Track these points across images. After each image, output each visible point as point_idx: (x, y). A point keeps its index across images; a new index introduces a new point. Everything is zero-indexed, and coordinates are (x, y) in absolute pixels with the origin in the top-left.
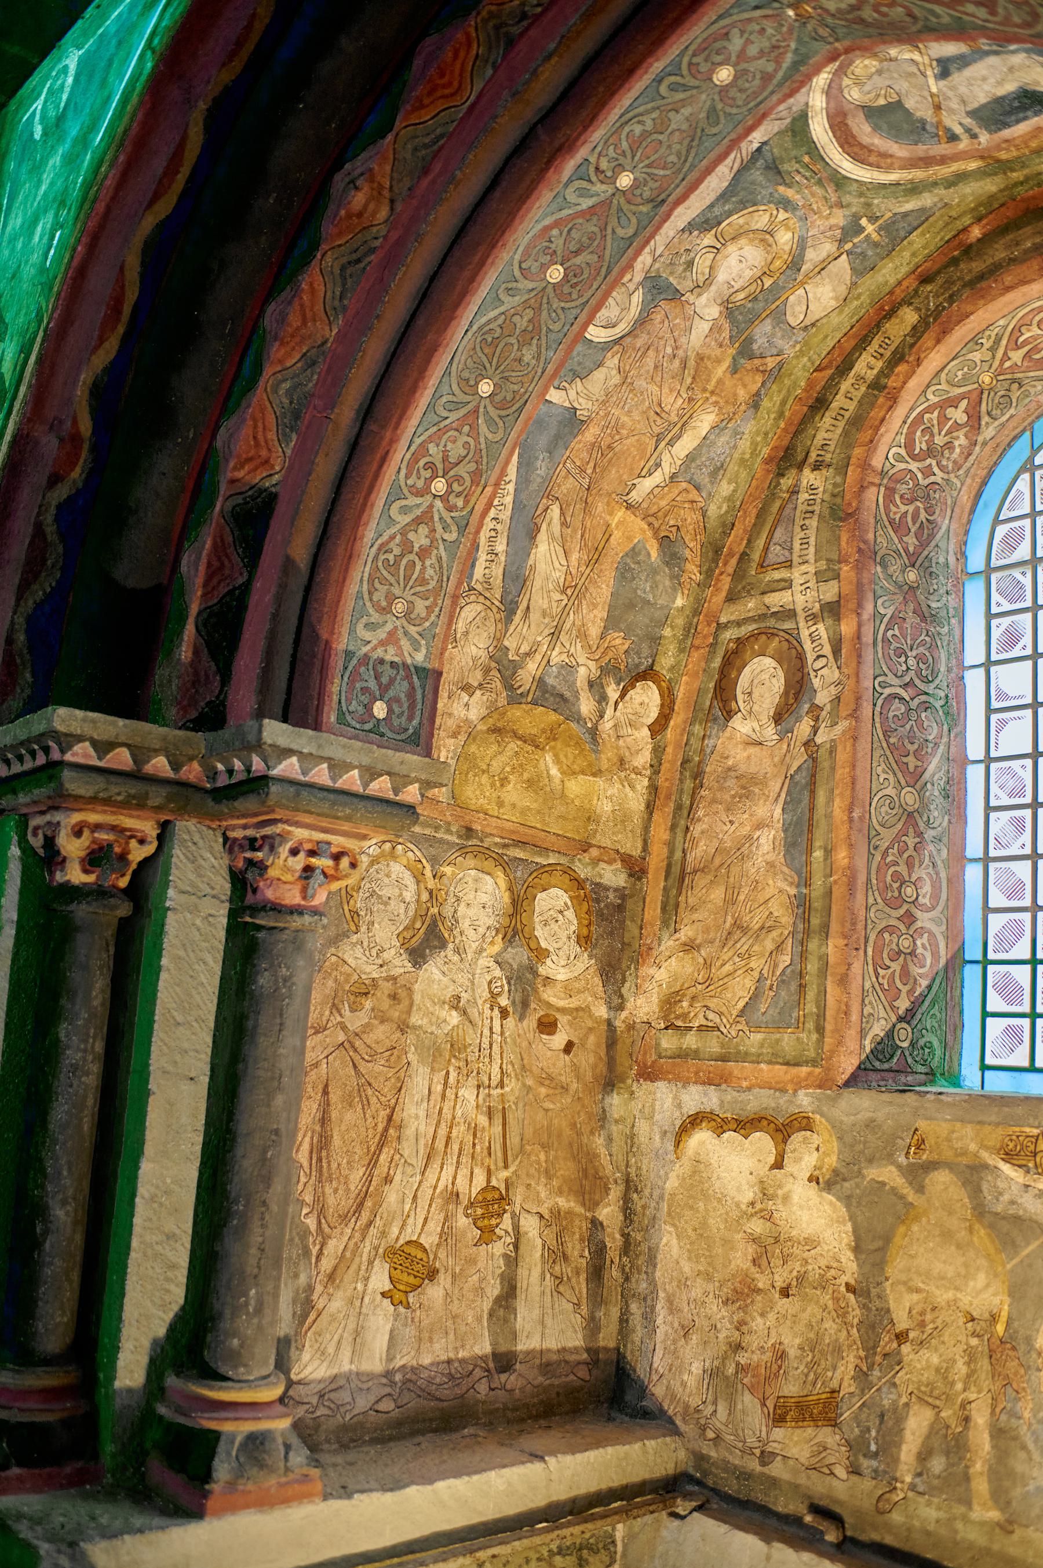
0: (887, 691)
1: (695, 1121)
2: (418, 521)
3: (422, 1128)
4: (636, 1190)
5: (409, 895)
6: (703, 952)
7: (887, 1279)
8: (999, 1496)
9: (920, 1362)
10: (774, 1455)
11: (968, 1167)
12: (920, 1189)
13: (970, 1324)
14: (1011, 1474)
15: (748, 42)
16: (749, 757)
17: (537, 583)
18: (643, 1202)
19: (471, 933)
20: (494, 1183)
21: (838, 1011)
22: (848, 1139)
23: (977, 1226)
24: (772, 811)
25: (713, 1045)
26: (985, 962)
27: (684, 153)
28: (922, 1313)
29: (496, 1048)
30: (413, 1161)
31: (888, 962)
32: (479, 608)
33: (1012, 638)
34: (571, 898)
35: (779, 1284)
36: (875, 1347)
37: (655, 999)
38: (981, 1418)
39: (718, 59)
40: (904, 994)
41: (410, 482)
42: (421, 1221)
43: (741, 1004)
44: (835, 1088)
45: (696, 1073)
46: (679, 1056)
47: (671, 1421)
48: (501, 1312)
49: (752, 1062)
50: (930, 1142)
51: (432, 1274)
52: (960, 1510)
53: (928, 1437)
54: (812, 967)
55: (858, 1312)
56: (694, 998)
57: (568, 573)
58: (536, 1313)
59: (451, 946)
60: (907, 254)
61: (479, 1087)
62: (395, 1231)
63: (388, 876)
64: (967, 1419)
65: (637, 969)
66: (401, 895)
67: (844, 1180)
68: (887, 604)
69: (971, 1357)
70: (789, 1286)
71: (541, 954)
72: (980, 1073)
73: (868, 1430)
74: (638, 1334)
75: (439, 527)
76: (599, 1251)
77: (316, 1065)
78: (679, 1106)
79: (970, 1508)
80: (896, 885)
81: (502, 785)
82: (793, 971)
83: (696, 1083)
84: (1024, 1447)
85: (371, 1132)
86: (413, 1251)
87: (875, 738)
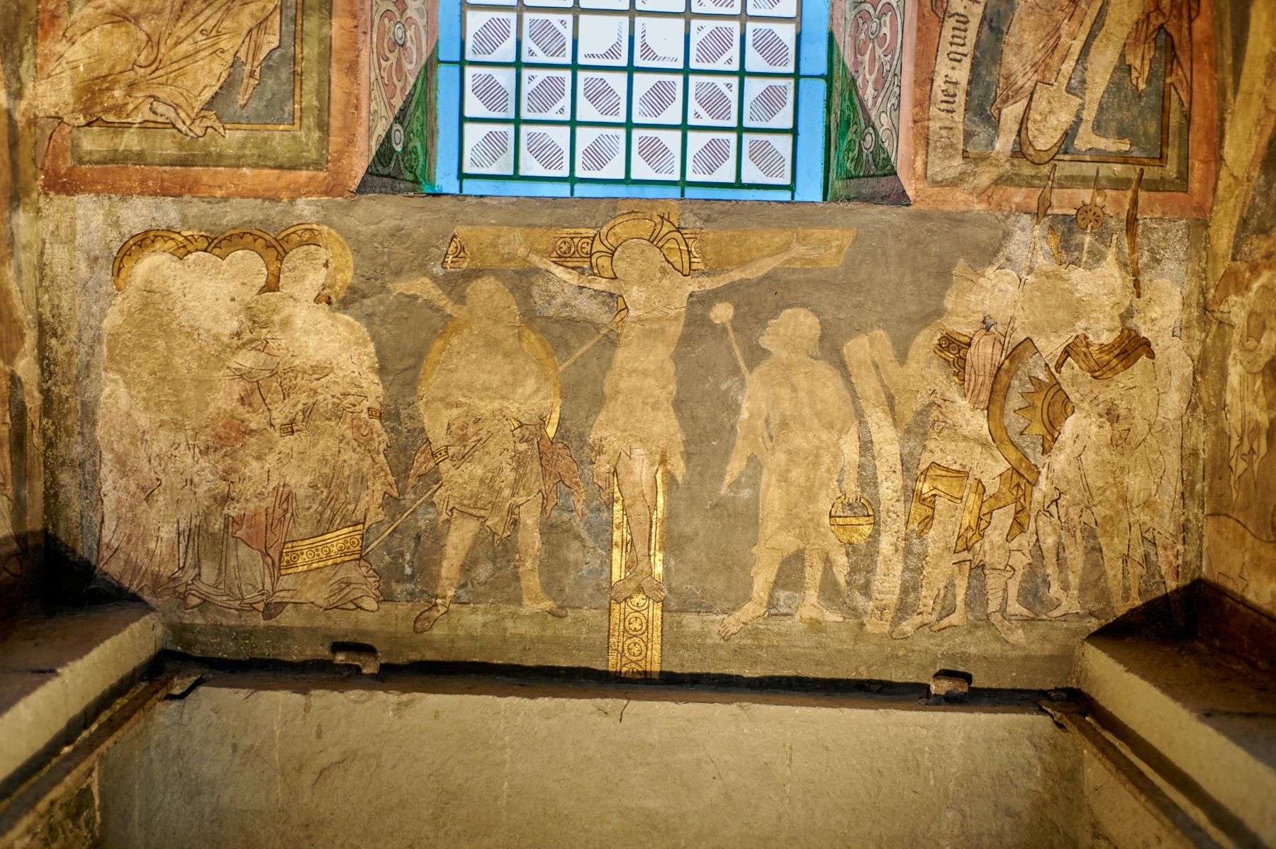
1: (143, 241)
4: (55, 335)
6: (144, 25)
8: (551, 586)
9: (462, 478)
10: (283, 604)
11: (516, 272)
12: (461, 300)
14: (565, 565)
18: (67, 347)
21: (347, 104)
22: (367, 251)
23: (527, 332)
25: (167, 146)
26: (462, 63)
28: (464, 427)
36: (407, 470)
37: (67, 86)
38: (530, 519)
40: (398, 92)
43: (207, 95)
44: (347, 194)
45: (143, 182)
46: (112, 161)
47: (136, 599)
49: (230, 166)
50: (472, 247)
52: (506, 609)
53: (473, 548)
54: (310, 51)
55: (385, 436)
56: (132, 86)
65: (35, 44)
67: (364, 297)
69: (520, 462)
70: (293, 421)
72: (457, 183)
73: (402, 555)
74: (75, 507)
76: (20, 414)
78: (116, 224)
79: (521, 605)
82: (283, 55)
83: (142, 194)
84: (578, 537)
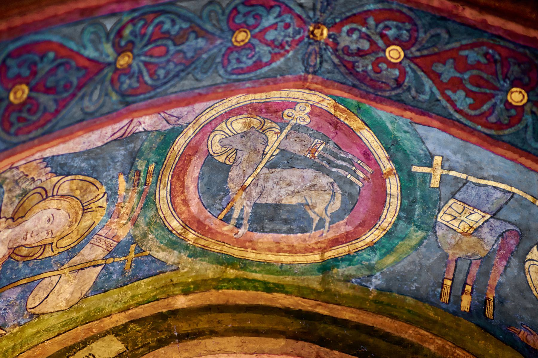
15: (274, 26)
27: (171, 75)
39: (251, 21)
60: (130, 293)
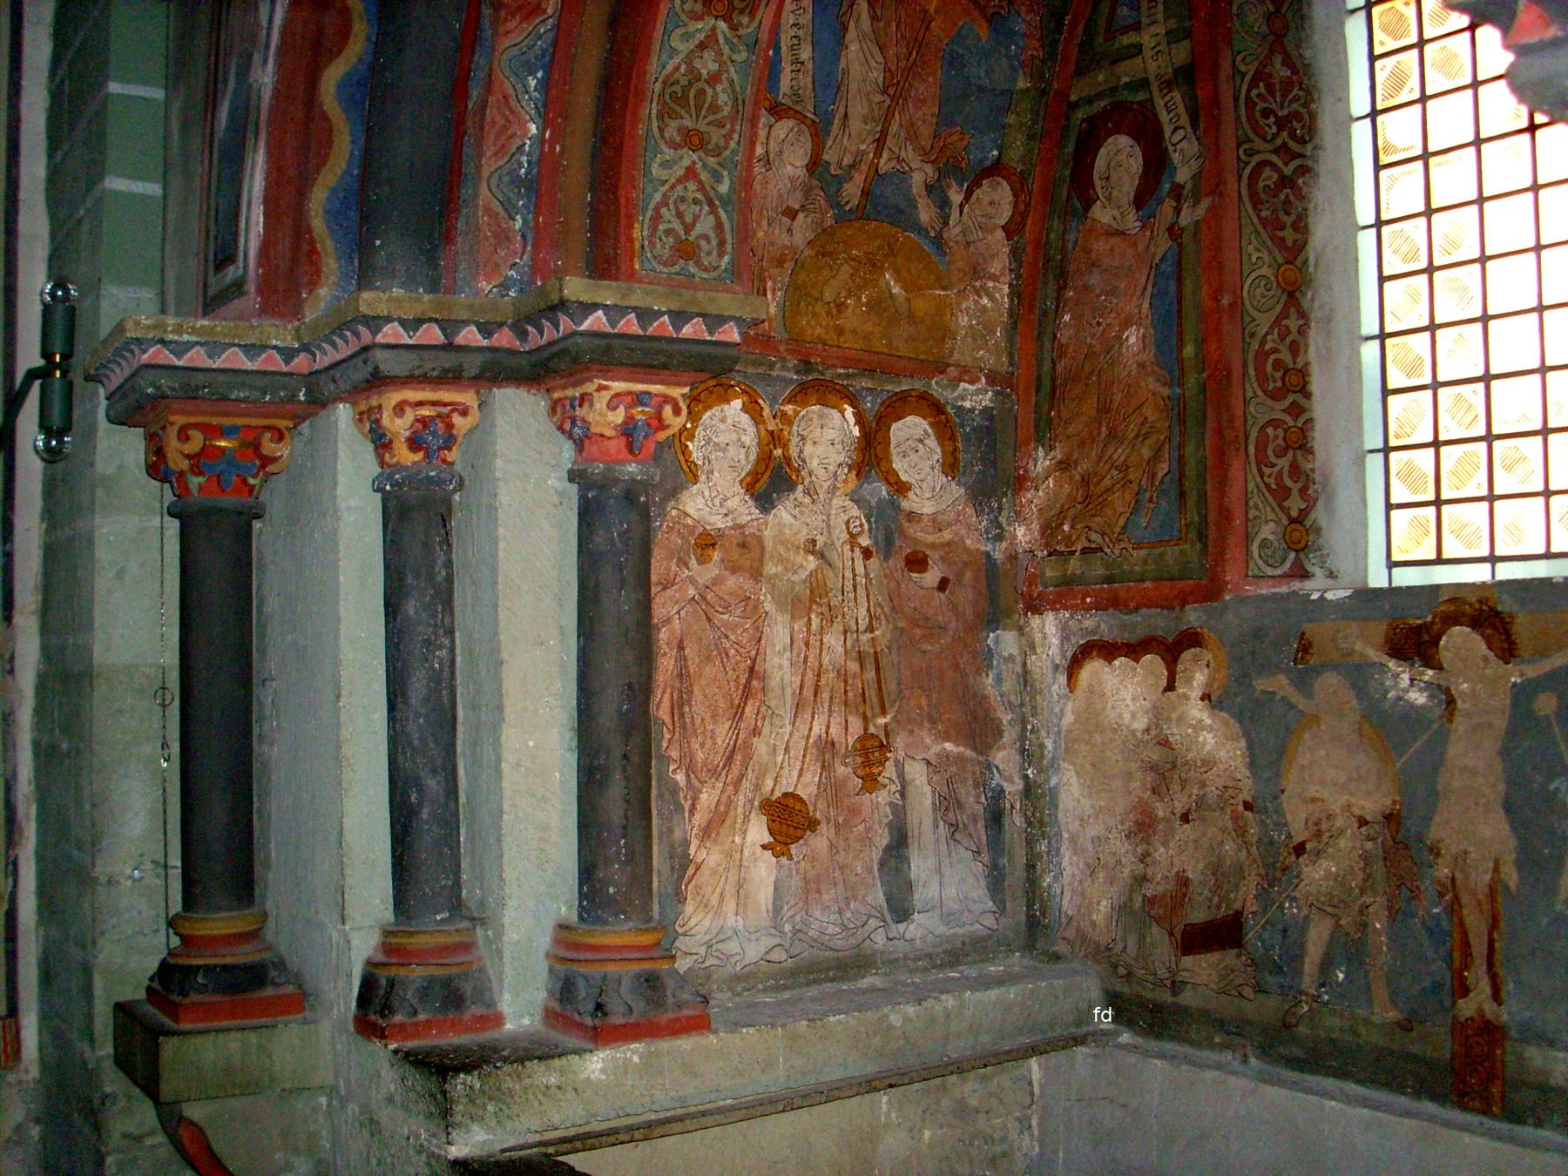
0: (1256, 159)
2: (702, 46)
3: (787, 678)
5: (750, 438)
7: (1283, 791)
13: (1363, 829)
16: (1112, 250)
17: (853, 87)
19: (821, 472)
20: (872, 730)
24: (1140, 307)
29: (861, 591)
30: (782, 712)
31: (1273, 460)
32: (791, 123)
33: (1398, 81)
34: (931, 425)
35: (1178, 812)
41: (687, 7)
42: (795, 773)
43: (1122, 521)
48: (893, 862)
51: (813, 825)
57: (887, 70)
58: (931, 862)
59: (800, 488)
61: (845, 632)
62: (769, 783)
63: (723, 420)
64: (1364, 925)
66: (739, 440)
68: (1248, 60)
70: (1189, 811)
71: (901, 488)
73: (1273, 947)
75: (726, 50)
77: (668, 621)
80: (1278, 375)
81: (839, 312)
85: (732, 684)
86: (791, 802)
87: (1243, 214)
